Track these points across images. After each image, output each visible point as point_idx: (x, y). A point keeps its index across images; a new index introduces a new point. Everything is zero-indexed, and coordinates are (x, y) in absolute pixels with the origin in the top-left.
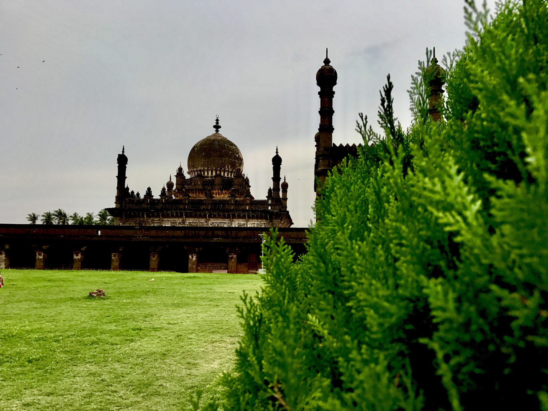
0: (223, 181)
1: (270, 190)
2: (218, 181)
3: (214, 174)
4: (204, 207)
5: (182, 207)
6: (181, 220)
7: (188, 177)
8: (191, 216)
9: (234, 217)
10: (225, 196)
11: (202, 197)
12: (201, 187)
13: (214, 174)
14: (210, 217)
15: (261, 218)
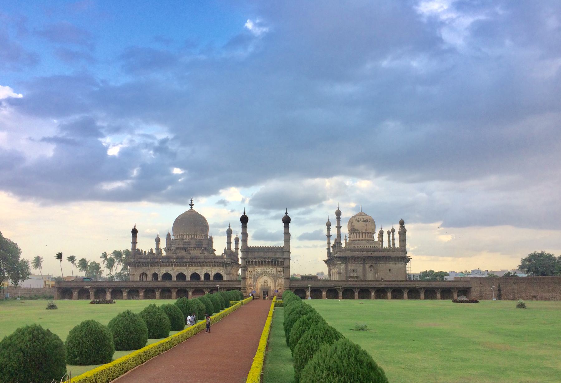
0: (196, 242)
1: (225, 249)
2: (193, 242)
3: (190, 237)
4: (184, 260)
5: (172, 260)
6: (170, 268)
7: (172, 237)
8: (178, 265)
9: (204, 265)
10: (196, 253)
11: (183, 253)
12: (182, 246)
13: (190, 237)
14: (189, 265)
15: (220, 266)
